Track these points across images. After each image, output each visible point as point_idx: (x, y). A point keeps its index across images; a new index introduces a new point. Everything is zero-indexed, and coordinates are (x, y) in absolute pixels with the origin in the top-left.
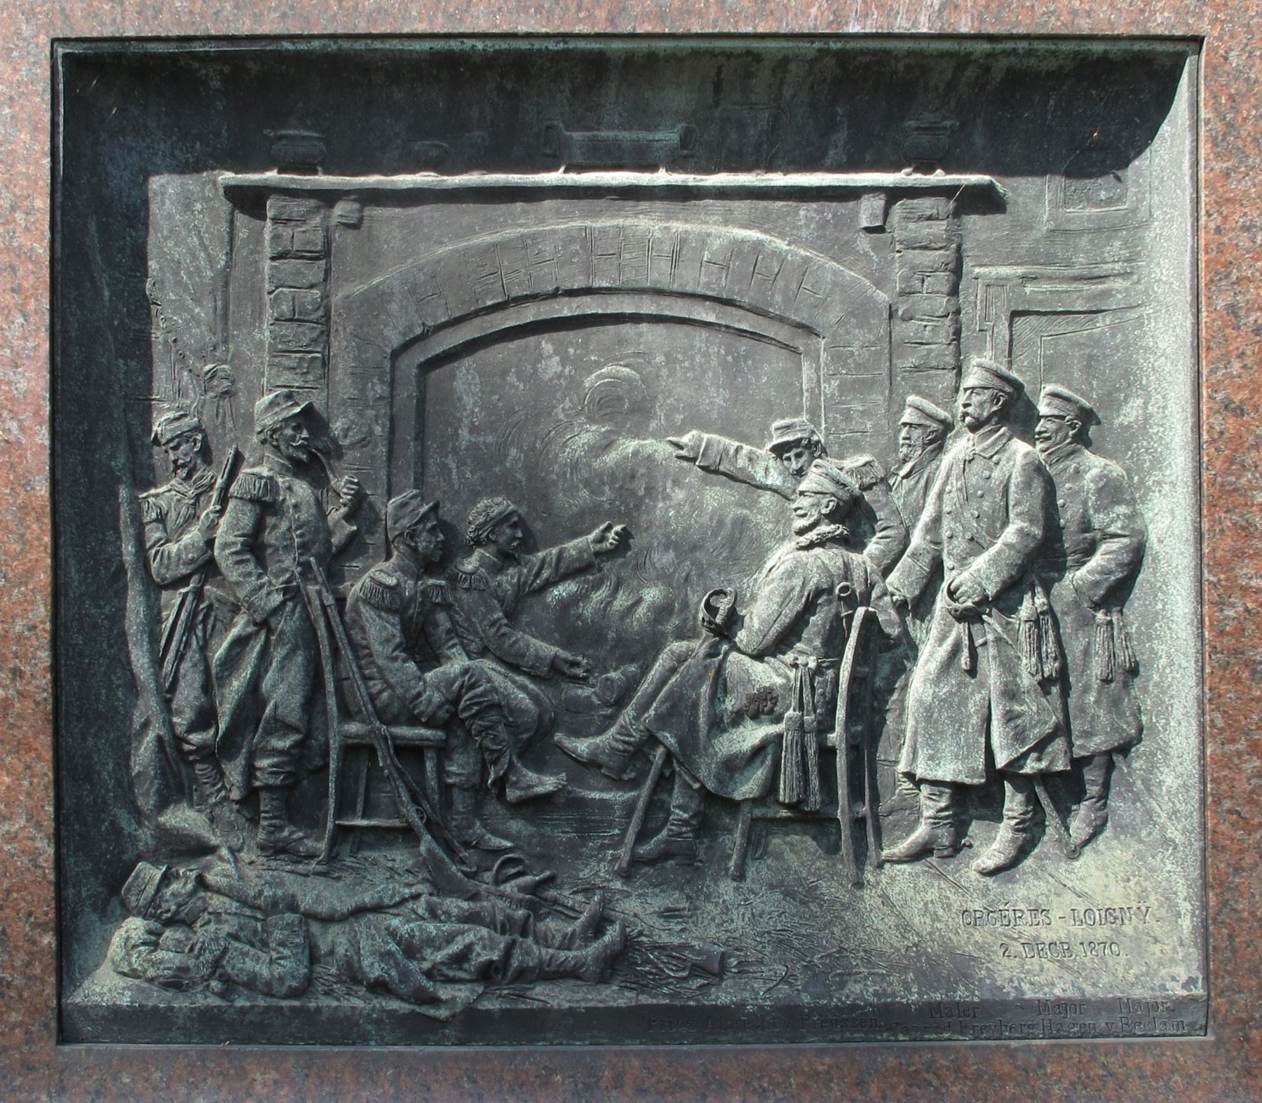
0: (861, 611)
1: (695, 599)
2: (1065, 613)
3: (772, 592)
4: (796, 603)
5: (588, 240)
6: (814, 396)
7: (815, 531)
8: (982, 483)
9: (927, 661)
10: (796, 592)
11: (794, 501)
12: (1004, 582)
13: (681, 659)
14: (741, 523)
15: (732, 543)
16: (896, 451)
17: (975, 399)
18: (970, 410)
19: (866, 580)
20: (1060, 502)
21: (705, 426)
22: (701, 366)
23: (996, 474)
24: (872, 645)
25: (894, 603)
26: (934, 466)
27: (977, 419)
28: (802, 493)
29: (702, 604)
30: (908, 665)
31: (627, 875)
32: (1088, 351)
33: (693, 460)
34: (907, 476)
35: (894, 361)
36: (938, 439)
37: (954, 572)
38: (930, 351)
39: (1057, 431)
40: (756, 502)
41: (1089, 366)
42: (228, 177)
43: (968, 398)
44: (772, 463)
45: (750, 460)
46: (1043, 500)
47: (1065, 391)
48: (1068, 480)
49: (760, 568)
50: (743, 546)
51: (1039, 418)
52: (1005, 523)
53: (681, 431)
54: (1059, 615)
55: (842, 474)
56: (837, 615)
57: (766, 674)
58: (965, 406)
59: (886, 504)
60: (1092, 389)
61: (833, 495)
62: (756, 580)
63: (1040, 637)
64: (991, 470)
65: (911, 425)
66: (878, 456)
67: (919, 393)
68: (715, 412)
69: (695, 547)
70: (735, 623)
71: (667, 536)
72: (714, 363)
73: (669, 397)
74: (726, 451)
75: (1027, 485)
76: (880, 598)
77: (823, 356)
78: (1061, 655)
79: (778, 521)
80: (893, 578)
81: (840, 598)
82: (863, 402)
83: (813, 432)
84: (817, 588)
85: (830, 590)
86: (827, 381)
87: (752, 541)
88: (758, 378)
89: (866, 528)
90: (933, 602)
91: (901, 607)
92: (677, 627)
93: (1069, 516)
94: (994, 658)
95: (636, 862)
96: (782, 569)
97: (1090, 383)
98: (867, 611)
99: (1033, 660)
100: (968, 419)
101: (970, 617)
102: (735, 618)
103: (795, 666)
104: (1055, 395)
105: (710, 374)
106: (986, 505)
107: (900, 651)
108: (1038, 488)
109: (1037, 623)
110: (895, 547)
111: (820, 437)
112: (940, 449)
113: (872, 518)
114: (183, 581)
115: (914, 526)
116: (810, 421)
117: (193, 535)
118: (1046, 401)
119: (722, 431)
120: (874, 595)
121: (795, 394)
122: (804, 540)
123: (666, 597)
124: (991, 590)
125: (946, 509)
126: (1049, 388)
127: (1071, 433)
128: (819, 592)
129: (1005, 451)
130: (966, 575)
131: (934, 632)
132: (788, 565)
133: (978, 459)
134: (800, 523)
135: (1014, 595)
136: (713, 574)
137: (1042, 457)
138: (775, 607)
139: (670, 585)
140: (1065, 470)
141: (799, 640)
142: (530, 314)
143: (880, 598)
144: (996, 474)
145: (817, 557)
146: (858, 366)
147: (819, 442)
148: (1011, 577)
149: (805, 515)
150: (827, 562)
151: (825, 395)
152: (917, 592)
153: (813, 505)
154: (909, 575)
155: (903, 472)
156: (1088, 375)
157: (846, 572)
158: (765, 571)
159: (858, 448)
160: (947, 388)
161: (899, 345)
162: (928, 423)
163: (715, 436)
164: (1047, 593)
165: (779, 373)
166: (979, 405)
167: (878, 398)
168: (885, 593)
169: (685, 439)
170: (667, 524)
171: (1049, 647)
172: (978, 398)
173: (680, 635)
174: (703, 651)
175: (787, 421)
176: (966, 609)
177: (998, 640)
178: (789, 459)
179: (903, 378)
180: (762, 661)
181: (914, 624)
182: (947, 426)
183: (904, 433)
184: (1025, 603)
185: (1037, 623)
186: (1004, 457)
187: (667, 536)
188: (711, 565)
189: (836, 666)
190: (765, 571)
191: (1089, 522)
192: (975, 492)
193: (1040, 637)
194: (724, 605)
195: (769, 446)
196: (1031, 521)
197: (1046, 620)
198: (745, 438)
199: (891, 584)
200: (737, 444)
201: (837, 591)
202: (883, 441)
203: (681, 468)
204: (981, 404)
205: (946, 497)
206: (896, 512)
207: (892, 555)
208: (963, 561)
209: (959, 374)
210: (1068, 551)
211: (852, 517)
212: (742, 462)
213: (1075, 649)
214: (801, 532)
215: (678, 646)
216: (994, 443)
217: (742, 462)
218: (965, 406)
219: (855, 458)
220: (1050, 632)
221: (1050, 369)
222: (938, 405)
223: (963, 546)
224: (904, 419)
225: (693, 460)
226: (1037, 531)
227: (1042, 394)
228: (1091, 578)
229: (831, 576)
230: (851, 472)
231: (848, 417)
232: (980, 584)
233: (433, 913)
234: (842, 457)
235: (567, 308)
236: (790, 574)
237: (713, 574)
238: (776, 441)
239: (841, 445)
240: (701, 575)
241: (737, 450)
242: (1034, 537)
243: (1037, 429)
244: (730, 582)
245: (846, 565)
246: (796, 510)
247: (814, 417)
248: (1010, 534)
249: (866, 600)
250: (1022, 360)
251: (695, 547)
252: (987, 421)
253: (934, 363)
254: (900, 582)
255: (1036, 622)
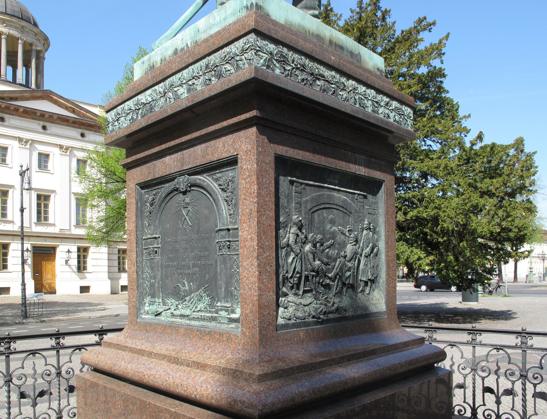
5: (329, 195)
31: (334, 296)
42: (289, 178)
57: (349, 264)
95: (336, 294)
114: (285, 247)
117: (286, 240)
142: (323, 206)
233: (317, 303)
235: (327, 206)
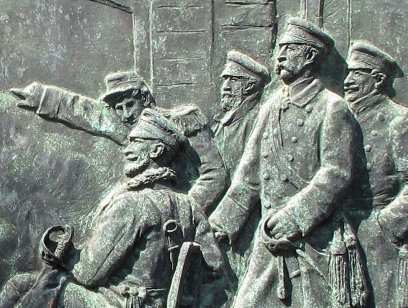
0: (186, 245)
1: (36, 235)
2: (372, 248)
3: (105, 228)
4: (128, 239)
6: (144, 52)
7: (145, 174)
8: (296, 130)
9: (246, 291)
10: (127, 229)
11: (125, 146)
12: (316, 220)
13: (23, 289)
14: (78, 167)
15: (69, 184)
16: (218, 101)
17: (290, 54)
18: (285, 63)
19: (191, 217)
20: (367, 147)
21: (44, 78)
22: (41, 24)
23: (309, 121)
24: (196, 277)
25: (216, 239)
26: (252, 115)
27: (291, 72)
28: (132, 139)
29: (42, 240)
30: (229, 295)
32: (392, 10)
33: (34, 109)
34: (228, 123)
35: (216, 19)
36: (256, 89)
37: (271, 211)
38: (249, 10)
39: (364, 83)
40: (91, 147)
41: (393, 24)
43: (284, 53)
44: (105, 111)
45: (86, 109)
46: (352, 146)
47: (372, 47)
48: (374, 127)
49: (94, 206)
50: (79, 187)
51: (348, 71)
52: (317, 166)
53: (23, 83)
54: (366, 249)
55: (169, 122)
56: (165, 249)
58: (281, 60)
59: (209, 149)
60: (396, 45)
61: (161, 140)
62: (91, 218)
63: (348, 270)
64: (304, 118)
65: (231, 77)
66: (202, 105)
67: (239, 48)
68: (54, 65)
69: (35, 188)
70: (72, 256)
71: (10, 178)
72: (53, 21)
73: (12, 52)
74: (64, 100)
75: (337, 131)
76: (203, 234)
77: (152, 14)
78: (368, 285)
79: (111, 165)
80: (215, 215)
81: (167, 234)
82: (188, 56)
83: (143, 84)
84: (146, 225)
85: (158, 227)
86: (156, 37)
87: (87, 182)
88: (93, 34)
89: (190, 170)
90: (252, 238)
91: (223, 242)
92: (20, 260)
93: (375, 160)
94: (307, 288)
96: (115, 208)
97: (394, 39)
98: (191, 246)
99: (343, 290)
100: (283, 72)
101: (285, 251)
102: (71, 254)
103: (127, 295)
104: (362, 50)
105: (50, 31)
106: (299, 150)
107: (221, 282)
108: (346, 134)
109: (346, 256)
110: (217, 188)
111: (149, 88)
112: (258, 99)
113: (197, 162)
115: (234, 169)
116: (140, 73)
118: (354, 55)
119: (59, 83)
120: (198, 232)
121: (126, 49)
122: (134, 181)
123: (9, 233)
124: (304, 227)
125: (264, 153)
126: (357, 44)
127: (377, 84)
128: (148, 229)
129: (316, 101)
130: (281, 213)
131: (253, 265)
132: (120, 204)
133: (292, 108)
134: (131, 166)
135: (325, 231)
136: (52, 212)
137: (351, 106)
138: (108, 242)
139: (13, 222)
140: (371, 118)
141: (130, 273)
143: (203, 234)
144: (309, 121)
145: (146, 197)
146: (184, 24)
147: (148, 92)
148: (323, 215)
149: (135, 159)
150: (155, 201)
151: (154, 50)
152: (237, 229)
153: (142, 150)
154: (230, 213)
155: (224, 120)
156: (392, 30)
157: (172, 211)
158: (99, 210)
159: (183, 98)
160: (264, 43)
161: (221, 5)
162: (247, 75)
163: (54, 88)
164: (355, 229)
165: (113, 29)
166: (293, 59)
167: (202, 53)
168: (208, 229)
169: (27, 90)
170: (11, 167)
171: (357, 278)
172: (293, 53)
173: (22, 269)
174: (43, 282)
175: (119, 74)
176: (281, 244)
177: (311, 272)
178: (121, 108)
179: (225, 35)
180: (97, 291)
181: (235, 257)
182: (264, 78)
183: (225, 84)
184: (335, 239)
185: (346, 256)
186: (316, 106)
187: (10, 178)
188: (50, 204)
189: (164, 295)
190: (99, 210)
191: (393, 165)
192: (290, 138)
193: (348, 270)
194: (62, 240)
195: (103, 96)
196: (341, 165)
197: (354, 253)
198: (80, 89)
199: (213, 221)
200: (73, 94)
201: (164, 228)
202: (206, 92)
203: (23, 116)
204: (295, 59)
205: (263, 142)
206: (218, 156)
207: (214, 196)
208: (279, 200)
209: (275, 29)
210: (374, 192)
211: (178, 161)
212: (78, 111)
213: (380, 280)
214: (132, 174)
215: (20, 278)
216: (307, 94)
217: (78, 111)
218: (281, 60)
219: (181, 107)
220: (358, 265)
221: (358, 26)
222: (256, 59)
223: (279, 186)
224: (225, 72)
225: (34, 109)
226: (346, 173)
227: (351, 49)
228: (394, 215)
229: (159, 214)
230: (177, 120)
231: (174, 70)
232: (294, 221)
234: (169, 107)
236: (122, 212)
237: (52, 212)
238: (109, 92)
239: (168, 95)
240: (41, 213)
241: (74, 100)
242: (343, 178)
243: (346, 81)
244: (67, 219)
245: (173, 205)
246: (127, 154)
247: (144, 71)
248: (321, 176)
249: (191, 235)
250: (333, 18)
251: (35, 188)
252: (301, 73)
253: (252, 21)
254: (221, 220)
255: (345, 255)
